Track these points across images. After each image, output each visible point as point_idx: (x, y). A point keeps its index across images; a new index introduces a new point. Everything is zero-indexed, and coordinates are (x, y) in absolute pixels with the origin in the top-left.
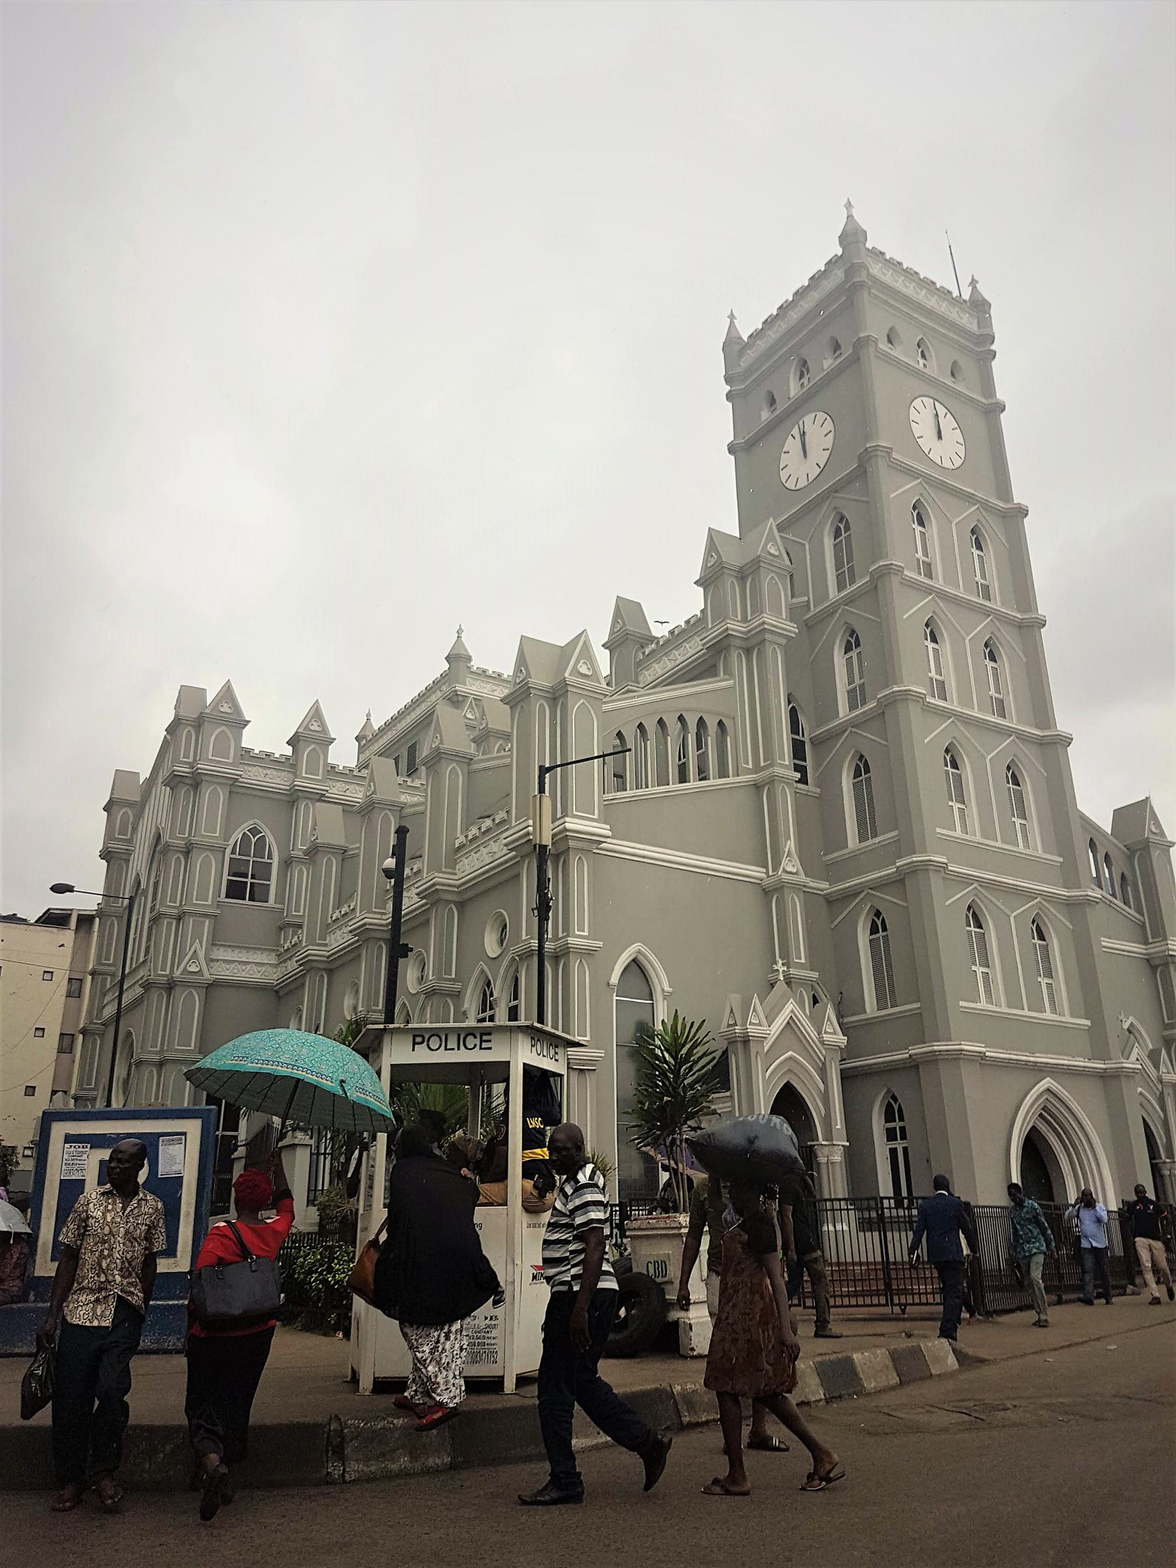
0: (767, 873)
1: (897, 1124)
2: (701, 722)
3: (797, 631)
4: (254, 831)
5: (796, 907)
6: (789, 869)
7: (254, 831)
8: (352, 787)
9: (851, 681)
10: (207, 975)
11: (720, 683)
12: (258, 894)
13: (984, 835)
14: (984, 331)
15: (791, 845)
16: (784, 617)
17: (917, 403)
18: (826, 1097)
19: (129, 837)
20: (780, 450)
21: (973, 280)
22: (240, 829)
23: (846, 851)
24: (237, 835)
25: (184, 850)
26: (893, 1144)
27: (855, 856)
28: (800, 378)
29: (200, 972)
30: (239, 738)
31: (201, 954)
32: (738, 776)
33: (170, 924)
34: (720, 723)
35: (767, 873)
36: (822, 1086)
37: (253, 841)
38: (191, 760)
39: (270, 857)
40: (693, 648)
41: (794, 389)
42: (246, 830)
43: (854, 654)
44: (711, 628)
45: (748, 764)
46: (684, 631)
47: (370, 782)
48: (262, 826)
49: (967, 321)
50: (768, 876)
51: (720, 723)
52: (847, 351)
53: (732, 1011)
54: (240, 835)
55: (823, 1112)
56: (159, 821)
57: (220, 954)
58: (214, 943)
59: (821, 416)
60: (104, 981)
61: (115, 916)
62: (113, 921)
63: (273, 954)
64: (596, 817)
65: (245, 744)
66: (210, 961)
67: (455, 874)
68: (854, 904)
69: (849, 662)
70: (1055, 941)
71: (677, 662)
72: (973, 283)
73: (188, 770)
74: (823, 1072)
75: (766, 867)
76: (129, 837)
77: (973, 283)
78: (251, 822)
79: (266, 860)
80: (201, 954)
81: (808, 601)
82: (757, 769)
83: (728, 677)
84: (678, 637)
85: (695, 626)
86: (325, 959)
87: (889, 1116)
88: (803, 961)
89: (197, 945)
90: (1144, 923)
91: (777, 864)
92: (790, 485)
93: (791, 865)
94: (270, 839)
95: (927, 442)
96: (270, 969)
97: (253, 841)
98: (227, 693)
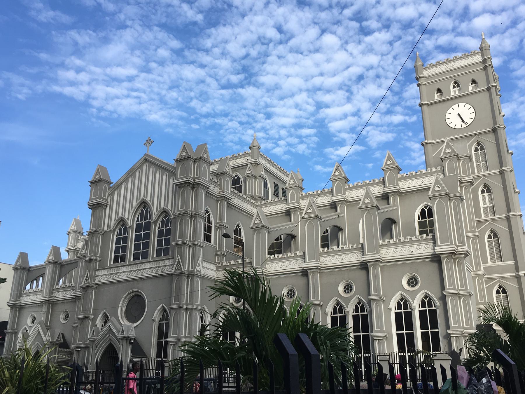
9: (485, 203)
10: (203, 273)
25: (190, 216)
29: (200, 271)
33: (187, 248)
35: (473, 269)
39: (211, 224)
43: (486, 195)
59: (468, 106)
61: (101, 234)
63: (215, 266)
73: (192, 181)
76: (106, 198)
86: (267, 274)
92: (452, 125)
94: (211, 216)
98: (203, 147)
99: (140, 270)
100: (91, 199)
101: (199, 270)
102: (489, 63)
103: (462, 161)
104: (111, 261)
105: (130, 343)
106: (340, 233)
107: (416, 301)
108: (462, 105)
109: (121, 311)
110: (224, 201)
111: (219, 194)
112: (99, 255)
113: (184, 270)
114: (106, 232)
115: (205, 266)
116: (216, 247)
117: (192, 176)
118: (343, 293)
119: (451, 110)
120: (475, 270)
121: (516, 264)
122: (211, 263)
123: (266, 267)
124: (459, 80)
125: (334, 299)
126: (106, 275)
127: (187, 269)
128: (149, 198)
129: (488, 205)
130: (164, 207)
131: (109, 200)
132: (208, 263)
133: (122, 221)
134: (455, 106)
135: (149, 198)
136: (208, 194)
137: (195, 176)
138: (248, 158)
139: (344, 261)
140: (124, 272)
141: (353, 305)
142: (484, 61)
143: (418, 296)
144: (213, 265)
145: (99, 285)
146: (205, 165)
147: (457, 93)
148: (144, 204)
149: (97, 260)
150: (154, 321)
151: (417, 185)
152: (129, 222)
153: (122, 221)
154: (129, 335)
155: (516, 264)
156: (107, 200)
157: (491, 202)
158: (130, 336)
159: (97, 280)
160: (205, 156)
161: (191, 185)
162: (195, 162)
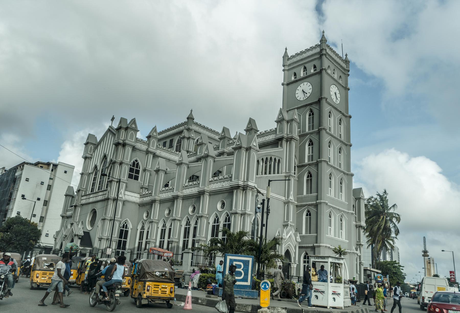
0: (285, 199)
1: (306, 260)
2: (275, 159)
3: (299, 139)
4: (136, 161)
5: (291, 207)
6: (291, 199)
7: (136, 161)
8: (161, 152)
9: (309, 153)
11: (279, 149)
12: (136, 178)
13: (334, 197)
14: (348, 69)
17: (332, 86)
18: (295, 253)
19: (92, 153)
21: (346, 54)
23: (303, 195)
24: (132, 161)
26: (305, 264)
27: (305, 197)
28: (304, 72)
29: (122, 198)
30: (136, 135)
31: (123, 193)
33: (115, 183)
34: (279, 160)
36: (294, 251)
37: (136, 163)
38: (123, 139)
39: (139, 168)
40: (271, 137)
41: (302, 74)
43: (311, 147)
44: (278, 134)
46: (269, 132)
47: (180, 157)
48: (138, 160)
49: (344, 65)
50: (286, 200)
51: (279, 160)
52: (318, 70)
53: (279, 232)
55: (294, 256)
56: (105, 152)
57: (127, 193)
58: (126, 190)
59: (309, 84)
60: (82, 193)
62: (85, 176)
63: (139, 195)
64: (254, 182)
65: (137, 137)
66: (125, 195)
67: (209, 188)
68: (303, 208)
69: (309, 148)
70: (344, 222)
71: (266, 140)
72: (346, 55)
73: (122, 142)
75: (285, 197)
76: (92, 153)
77: (346, 55)
78: (135, 158)
79: (138, 169)
80: (123, 193)
81: (300, 130)
82: (286, 173)
83: (281, 148)
84: (266, 133)
87: (305, 257)
88: (291, 221)
89: (122, 190)
90: (356, 217)
91: (288, 197)
92: (298, 98)
93: (291, 198)
94: (140, 163)
95: (333, 97)
96: (138, 199)
97: (136, 163)
98: (134, 121)
99: (97, 196)
100: (84, 154)
101: (121, 197)
102: (324, 52)
103: (290, 123)
104: (89, 192)
105: (79, 238)
106: (220, 174)
107: (221, 217)
108: (305, 83)
109: (88, 221)
112: (84, 188)
113: (110, 196)
114: (89, 174)
115: (130, 195)
117: (123, 139)
118: (191, 212)
119: (299, 88)
120: (286, 199)
121: (317, 196)
122: (136, 193)
124: (306, 65)
125: (186, 216)
126: (85, 199)
127: (113, 196)
128: (107, 153)
129: (311, 154)
131: (93, 155)
132: (132, 193)
133: (96, 167)
134: (302, 85)
135: (107, 153)
136: (134, 149)
137: (125, 139)
138: (185, 126)
140: (92, 197)
141: (194, 220)
142: (321, 50)
143: (223, 215)
144: (137, 194)
145: (82, 205)
146: (133, 132)
147: (305, 74)
148: (105, 157)
149: (83, 191)
150: (98, 226)
151: (263, 141)
152: (98, 168)
153: (96, 167)
154: (78, 234)
155: (317, 196)
156: (92, 155)
157: (312, 153)
158: (79, 234)
159: (82, 202)
160: (133, 126)
161: (122, 145)
162: (126, 130)
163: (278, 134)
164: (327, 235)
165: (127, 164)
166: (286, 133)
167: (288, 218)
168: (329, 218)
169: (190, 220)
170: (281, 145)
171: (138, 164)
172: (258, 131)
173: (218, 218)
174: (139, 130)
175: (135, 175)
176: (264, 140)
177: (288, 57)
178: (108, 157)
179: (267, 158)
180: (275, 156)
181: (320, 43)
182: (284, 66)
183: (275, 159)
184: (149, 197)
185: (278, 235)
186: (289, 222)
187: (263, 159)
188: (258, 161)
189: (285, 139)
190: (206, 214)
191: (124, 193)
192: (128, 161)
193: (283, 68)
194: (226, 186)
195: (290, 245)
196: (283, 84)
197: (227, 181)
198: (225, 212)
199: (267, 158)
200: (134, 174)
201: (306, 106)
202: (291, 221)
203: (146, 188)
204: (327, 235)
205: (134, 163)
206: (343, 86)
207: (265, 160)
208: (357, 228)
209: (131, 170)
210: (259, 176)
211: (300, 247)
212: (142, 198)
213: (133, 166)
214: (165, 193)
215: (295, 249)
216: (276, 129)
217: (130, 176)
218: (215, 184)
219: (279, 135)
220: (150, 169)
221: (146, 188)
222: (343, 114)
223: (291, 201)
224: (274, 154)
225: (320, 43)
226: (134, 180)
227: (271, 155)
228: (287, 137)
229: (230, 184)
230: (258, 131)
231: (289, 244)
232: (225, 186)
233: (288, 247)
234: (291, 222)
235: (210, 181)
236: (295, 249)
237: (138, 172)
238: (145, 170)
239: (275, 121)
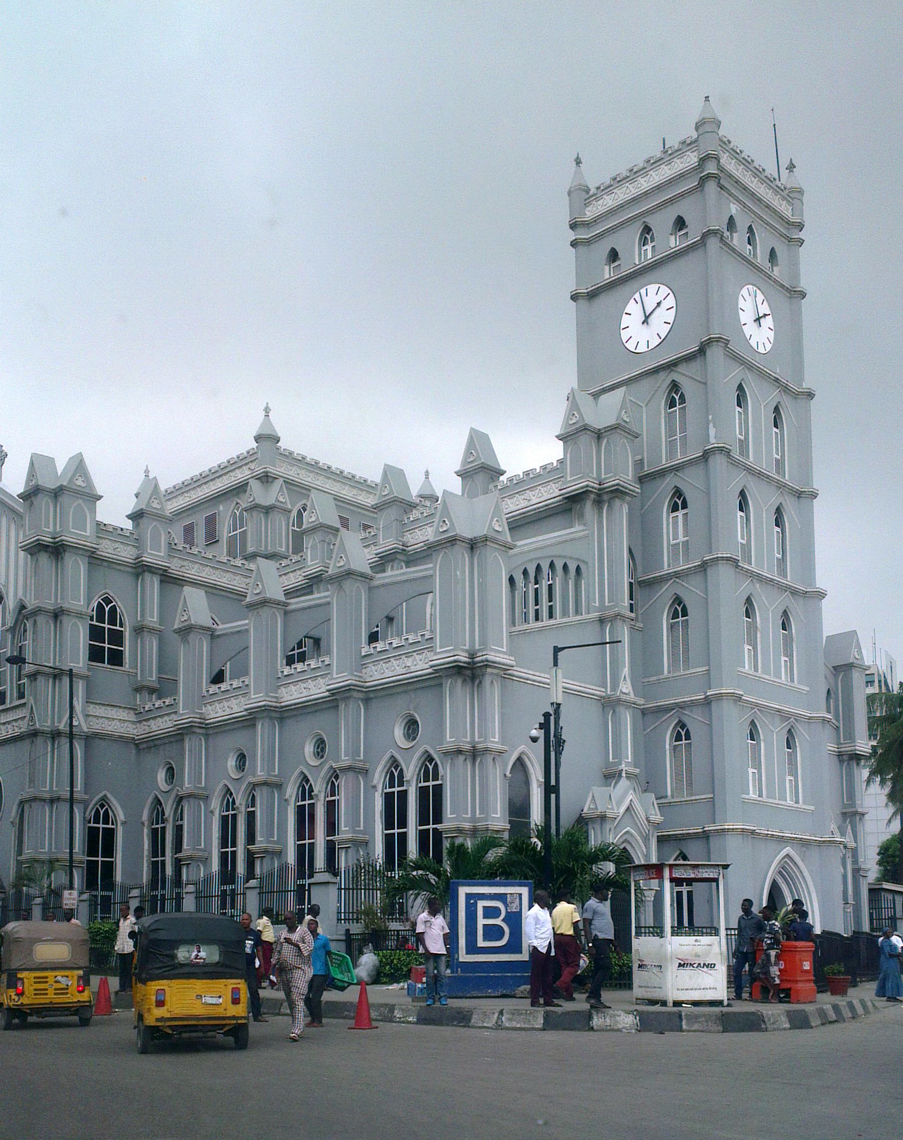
2: (565, 567)
5: (627, 718)
7: (108, 601)
12: (116, 658)
15: (626, 671)
16: (630, 478)
20: (620, 312)
22: (95, 599)
30: (93, 511)
32: (589, 613)
36: (644, 850)
37: (107, 609)
42: (100, 600)
45: (595, 603)
46: (539, 475)
54: (96, 604)
65: (100, 517)
74: (646, 840)
79: (118, 628)
85: (550, 473)
92: (631, 346)
93: (626, 687)
97: (107, 609)
103: (605, 440)
110: (146, 574)
111: (137, 561)
116: (136, 673)
123: (203, 711)
130: (23, 598)
139: (312, 692)
144: (126, 711)
163: (569, 479)
164: (743, 796)
165: (80, 615)
166: (595, 476)
167: (618, 754)
168: (749, 741)
169: (312, 781)
170: (581, 516)
171: (113, 610)
172: (502, 473)
173: (401, 770)
174: (100, 493)
175: (105, 643)
176: (523, 504)
177: (587, 191)
178: (7, 593)
179: (538, 568)
180: (564, 557)
181: (695, 135)
182: (573, 226)
183: (565, 567)
184: (166, 718)
185: (589, 809)
186: (623, 765)
187: (525, 572)
188: (511, 580)
189: (593, 496)
190: (360, 761)
191: (83, 710)
192: (82, 603)
193: (572, 236)
194: (418, 668)
195: (632, 835)
196: (574, 297)
197: (420, 652)
198: (421, 750)
199: (538, 568)
200: (107, 646)
201: (656, 371)
202: (630, 760)
203: (152, 691)
204: (743, 796)
205: (100, 608)
206: (783, 286)
207: (532, 574)
208: (841, 762)
209: (96, 633)
210: (518, 628)
211: (661, 840)
212: (145, 723)
213: (101, 618)
214: (220, 701)
215: (648, 847)
216: (561, 462)
217: (95, 655)
218: (381, 663)
219: (574, 485)
220: (157, 626)
221: (152, 691)
222: (786, 389)
223: (624, 697)
224: (557, 551)
225: (695, 135)
226: (109, 666)
227: (550, 556)
228: (599, 490)
229: (431, 663)
230: (502, 473)
231: (627, 832)
232: (413, 669)
233: (626, 841)
234: (627, 764)
235: (363, 654)
236: (648, 847)
237: (117, 638)
238: (139, 630)
239: (557, 437)
